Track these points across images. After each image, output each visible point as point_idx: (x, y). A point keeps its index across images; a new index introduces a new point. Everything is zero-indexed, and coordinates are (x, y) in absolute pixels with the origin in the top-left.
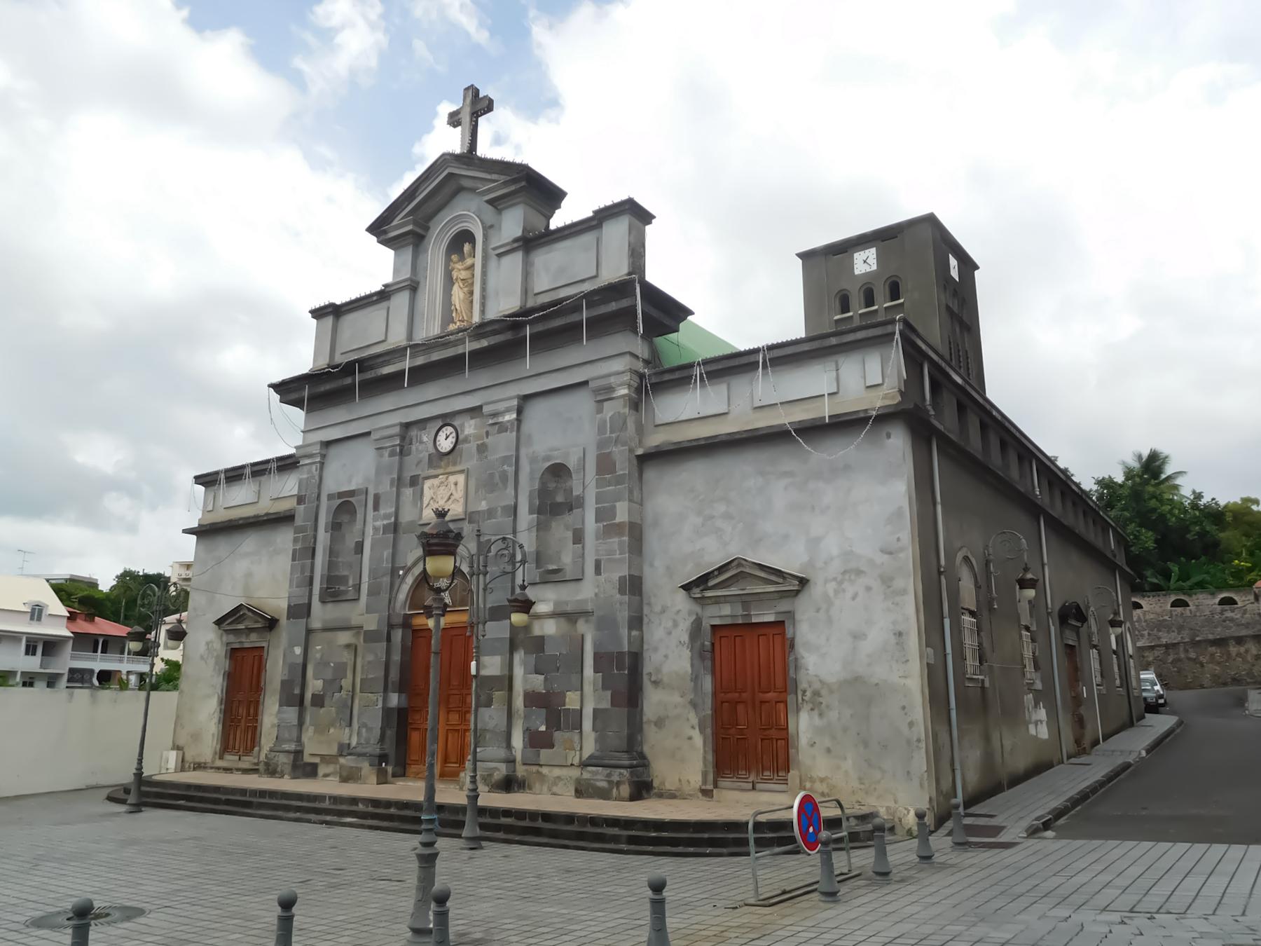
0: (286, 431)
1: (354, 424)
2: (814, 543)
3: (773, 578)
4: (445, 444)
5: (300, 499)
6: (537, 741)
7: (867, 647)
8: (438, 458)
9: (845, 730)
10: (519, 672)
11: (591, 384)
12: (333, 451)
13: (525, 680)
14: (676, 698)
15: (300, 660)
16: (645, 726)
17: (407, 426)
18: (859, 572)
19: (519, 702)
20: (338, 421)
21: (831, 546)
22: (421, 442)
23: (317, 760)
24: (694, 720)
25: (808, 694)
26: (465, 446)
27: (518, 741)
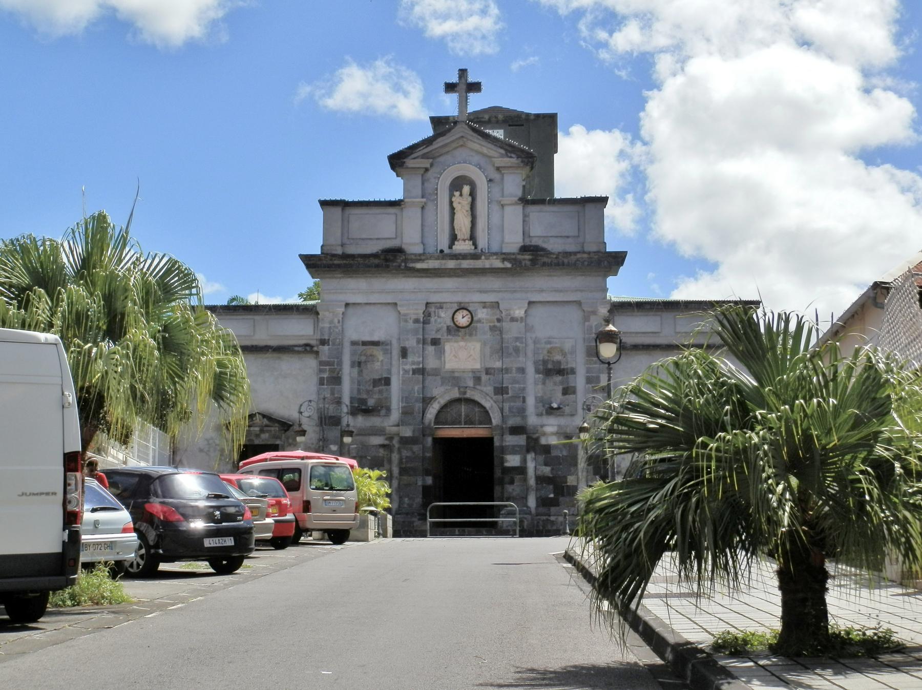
0: (293, 286)
6: (544, 502)
8: (455, 330)
10: (531, 465)
12: (351, 310)
19: (532, 482)
22: (439, 317)
26: (479, 325)
27: (532, 502)
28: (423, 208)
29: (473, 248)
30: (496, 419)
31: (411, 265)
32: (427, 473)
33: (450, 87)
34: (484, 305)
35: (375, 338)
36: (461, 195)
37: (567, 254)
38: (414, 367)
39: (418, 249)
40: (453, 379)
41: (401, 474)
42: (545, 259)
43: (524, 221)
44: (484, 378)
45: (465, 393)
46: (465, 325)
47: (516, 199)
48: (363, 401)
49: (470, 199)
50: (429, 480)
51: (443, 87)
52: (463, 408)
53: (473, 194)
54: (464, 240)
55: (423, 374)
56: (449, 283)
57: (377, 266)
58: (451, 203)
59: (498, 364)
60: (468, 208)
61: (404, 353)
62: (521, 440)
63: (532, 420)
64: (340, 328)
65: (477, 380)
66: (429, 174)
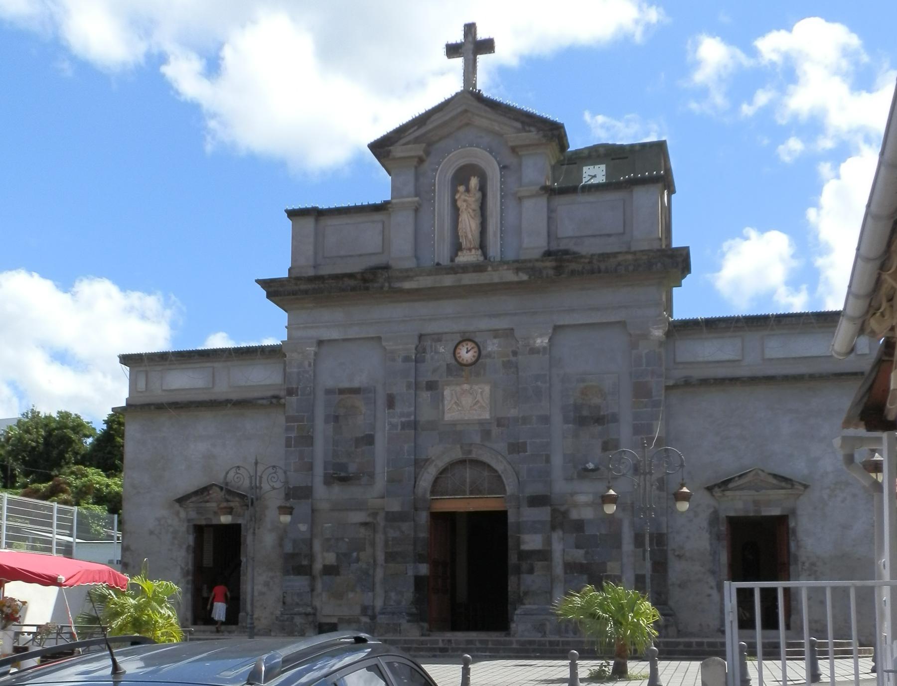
8: (458, 369)
10: (557, 548)
19: (559, 570)
20: (331, 322)
22: (437, 352)
25: (807, 565)
28: (416, 210)
29: (481, 259)
30: (510, 488)
31: (397, 285)
32: (420, 558)
33: (453, 50)
34: (495, 333)
35: (356, 384)
36: (468, 190)
37: (605, 256)
38: (403, 419)
39: (410, 264)
40: (454, 433)
41: (386, 561)
42: (573, 266)
43: (549, 218)
44: (495, 431)
45: (470, 452)
46: (470, 361)
47: (538, 187)
48: (343, 467)
49: (479, 195)
50: (424, 569)
51: (443, 51)
52: (468, 474)
53: (483, 189)
54: (470, 250)
55: (415, 429)
56: (449, 307)
57: (353, 289)
58: (454, 202)
59: (513, 412)
60: (475, 206)
61: (391, 402)
62: (543, 514)
63: (560, 486)
64: (311, 373)
65: (486, 434)
66: (426, 166)
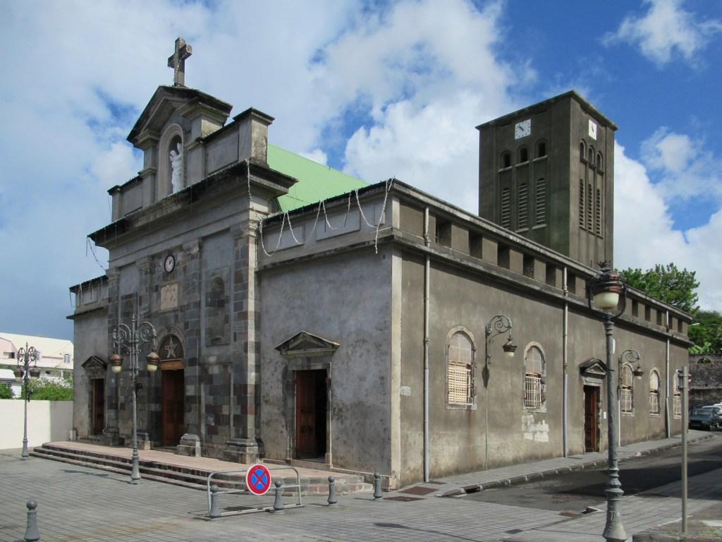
1: (129, 257)
2: (343, 323)
3: (320, 344)
4: (169, 267)
5: (110, 300)
7: (366, 385)
8: (168, 275)
9: (353, 431)
10: (203, 394)
11: (231, 230)
13: (206, 398)
14: (276, 411)
15: (114, 386)
16: (262, 425)
17: (153, 257)
18: (364, 341)
19: (203, 410)
21: (352, 324)
22: (160, 266)
23: (124, 437)
24: (284, 423)
25: (336, 410)
35: (131, 292)
